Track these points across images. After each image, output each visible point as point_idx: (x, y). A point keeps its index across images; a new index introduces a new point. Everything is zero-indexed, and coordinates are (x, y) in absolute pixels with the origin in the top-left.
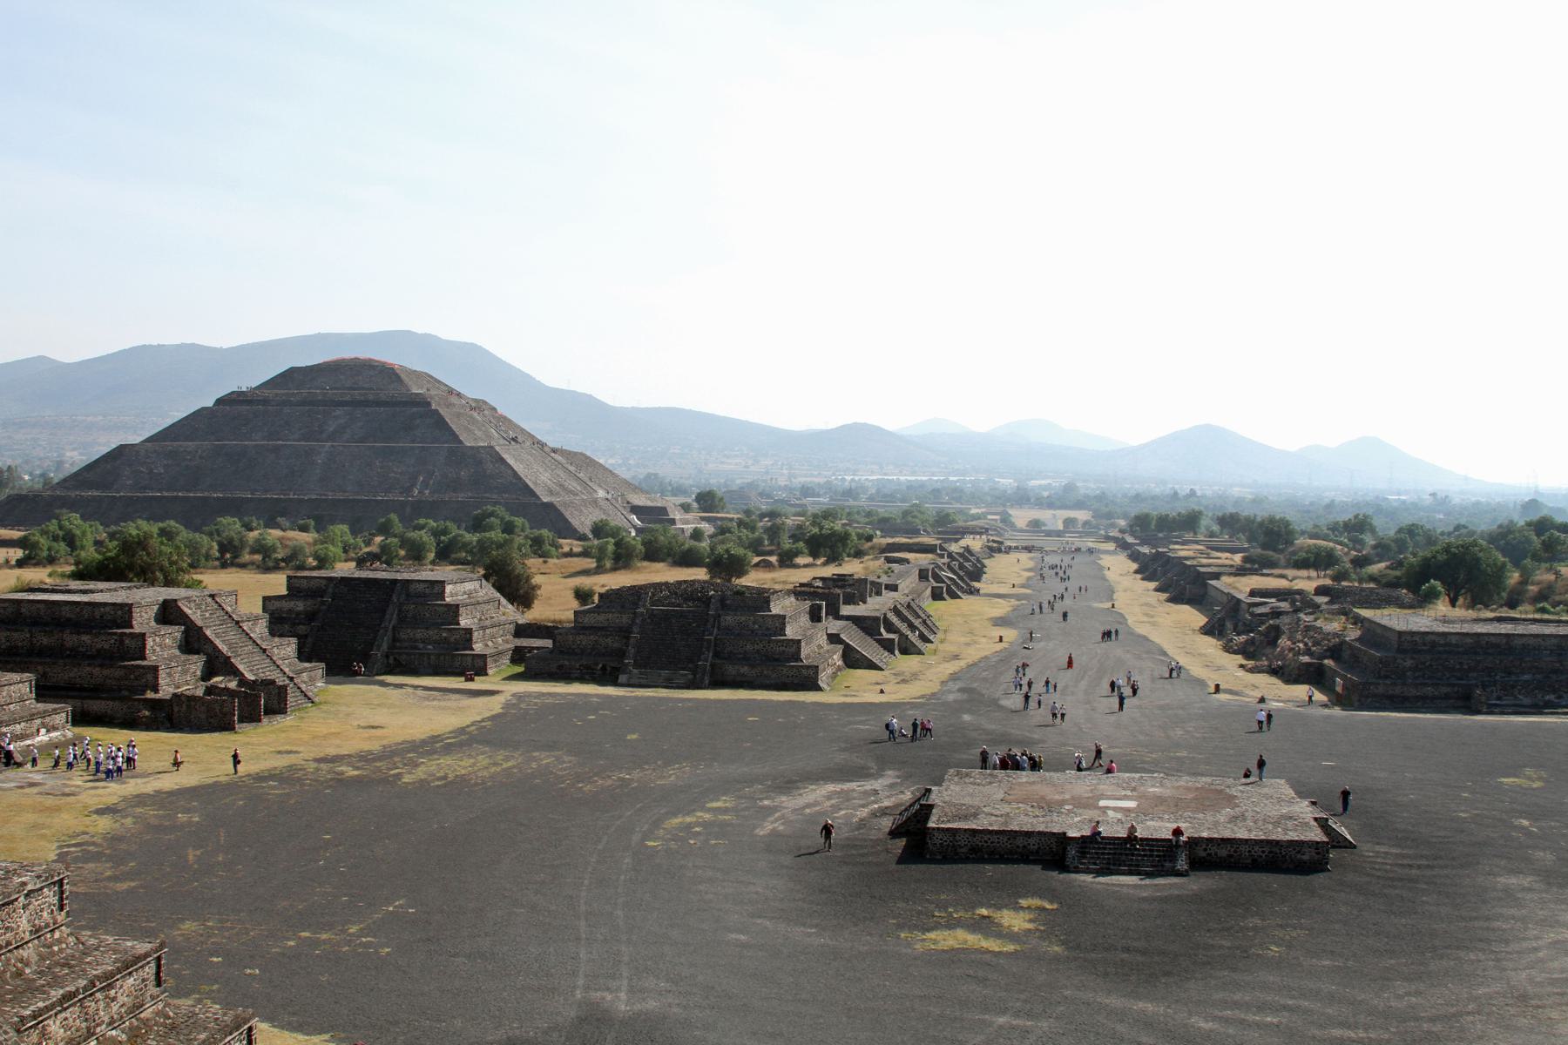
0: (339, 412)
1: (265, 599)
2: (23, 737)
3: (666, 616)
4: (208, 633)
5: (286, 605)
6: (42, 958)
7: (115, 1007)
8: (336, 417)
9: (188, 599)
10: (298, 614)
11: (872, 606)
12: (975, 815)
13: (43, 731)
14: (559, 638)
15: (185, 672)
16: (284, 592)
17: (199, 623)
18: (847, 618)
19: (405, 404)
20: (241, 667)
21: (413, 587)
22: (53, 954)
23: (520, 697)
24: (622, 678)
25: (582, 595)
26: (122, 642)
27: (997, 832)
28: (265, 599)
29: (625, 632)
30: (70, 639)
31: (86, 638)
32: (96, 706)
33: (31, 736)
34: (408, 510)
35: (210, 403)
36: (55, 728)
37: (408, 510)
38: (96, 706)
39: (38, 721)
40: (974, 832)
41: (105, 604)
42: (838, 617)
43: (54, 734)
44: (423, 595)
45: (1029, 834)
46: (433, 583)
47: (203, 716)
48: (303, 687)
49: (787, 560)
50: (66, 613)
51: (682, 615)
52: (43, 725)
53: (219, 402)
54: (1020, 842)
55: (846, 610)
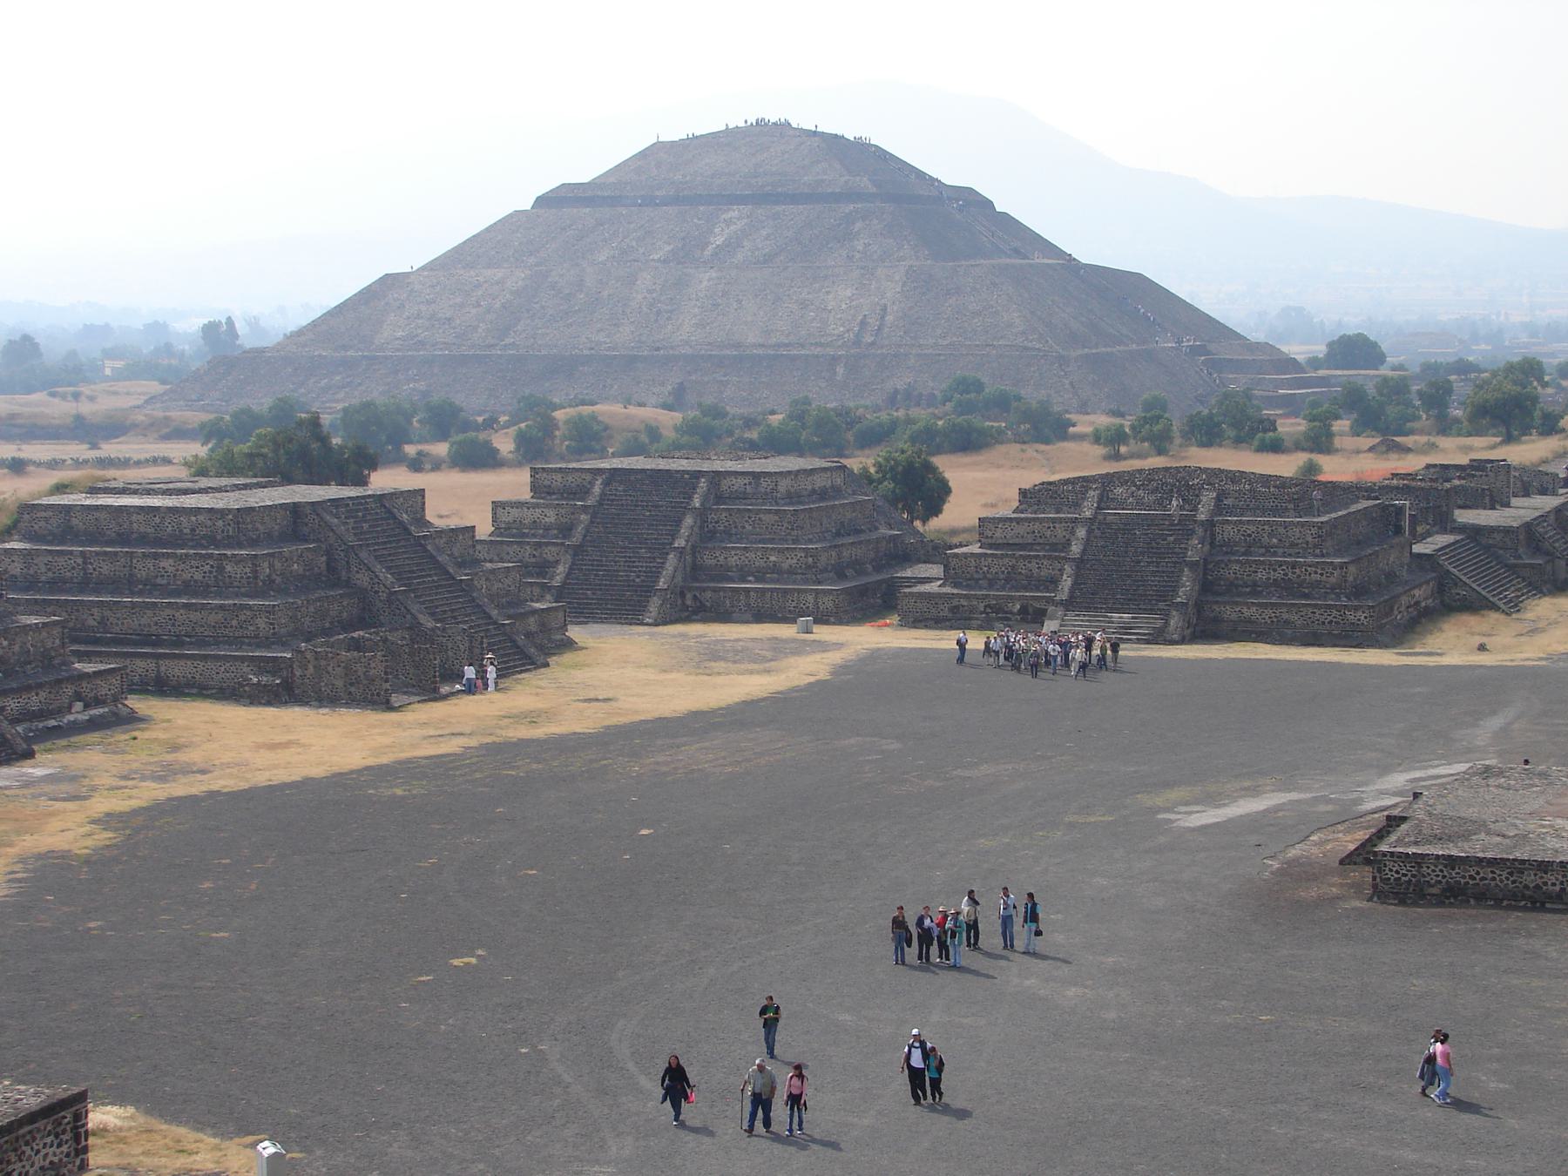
0: (734, 213)
1: (497, 506)
4: (363, 555)
5: (529, 516)
8: (728, 223)
9: (335, 502)
10: (547, 528)
12: (1466, 836)
13: (79, 706)
14: (953, 562)
16: (526, 495)
17: (351, 540)
18: (1463, 529)
19: (837, 198)
20: (415, 608)
21: (725, 484)
23: (874, 656)
26: (221, 569)
27: (1493, 862)
28: (497, 506)
32: (176, 670)
33: (60, 712)
34: (840, 370)
35: (527, 204)
36: (99, 702)
37: (840, 370)
39: (69, 690)
40: (1451, 861)
41: (198, 511)
42: (1444, 523)
44: (743, 497)
45: (1544, 866)
46: (756, 476)
47: (339, 683)
48: (521, 639)
50: (139, 525)
52: (78, 697)
53: (541, 201)
54: (1530, 879)
55: (1464, 516)
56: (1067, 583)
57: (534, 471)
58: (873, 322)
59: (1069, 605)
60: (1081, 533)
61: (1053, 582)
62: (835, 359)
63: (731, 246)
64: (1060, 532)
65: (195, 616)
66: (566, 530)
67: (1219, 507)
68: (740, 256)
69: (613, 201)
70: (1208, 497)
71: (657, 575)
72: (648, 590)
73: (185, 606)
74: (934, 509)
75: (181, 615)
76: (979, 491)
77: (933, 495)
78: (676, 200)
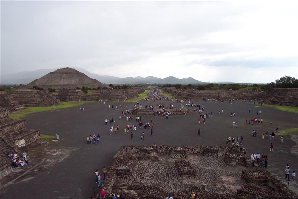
2: (17, 108)
3: (104, 93)
6: (5, 121)
7: (17, 128)
15: (40, 100)
22: (7, 120)
29: (99, 95)
30: (25, 96)
31: (27, 96)
32: (28, 104)
34: (73, 86)
35: (48, 74)
36: (22, 107)
38: (28, 104)
39: (19, 106)
43: (22, 108)
51: (106, 93)
52: (20, 106)
53: (49, 73)
61: (99, 97)
63: (64, 77)
64: (99, 93)
65: (29, 100)
66: (59, 94)
69: (55, 73)
73: (29, 99)
75: (28, 100)
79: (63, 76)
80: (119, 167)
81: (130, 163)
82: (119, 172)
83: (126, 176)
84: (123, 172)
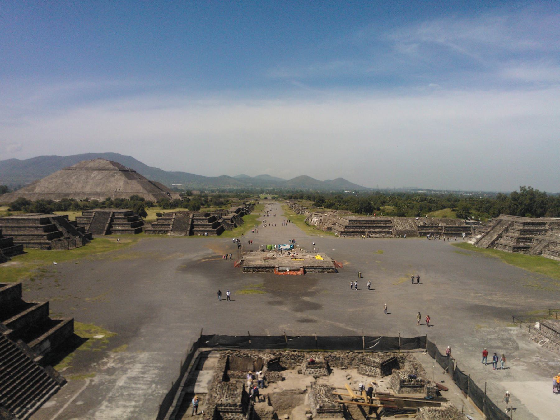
0: (95, 172)
1: (76, 218)
3: (180, 219)
11: (230, 216)
24: (169, 234)
25: (159, 215)
28: (76, 218)
49: (209, 206)
56: (171, 227)
57: (83, 213)
58: (118, 189)
59: (171, 231)
60: (173, 220)
62: (112, 194)
63: (95, 177)
67: (193, 216)
68: (97, 178)
70: (191, 215)
71: (104, 228)
72: (103, 230)
74: (145, 217)
76: (152, 215)
77: (145, 215)
78: (86, 170)
79: (93, 175)
80: (222, 399)
81: (238, 391)
82: (222, 409)
83: (232, 415)
84: (228, 407)
